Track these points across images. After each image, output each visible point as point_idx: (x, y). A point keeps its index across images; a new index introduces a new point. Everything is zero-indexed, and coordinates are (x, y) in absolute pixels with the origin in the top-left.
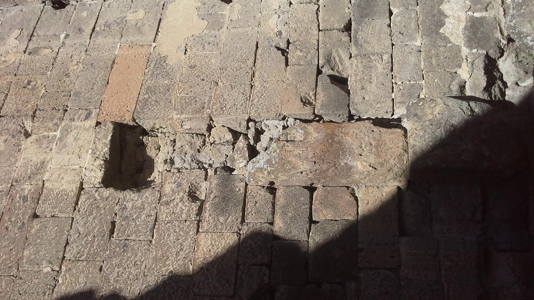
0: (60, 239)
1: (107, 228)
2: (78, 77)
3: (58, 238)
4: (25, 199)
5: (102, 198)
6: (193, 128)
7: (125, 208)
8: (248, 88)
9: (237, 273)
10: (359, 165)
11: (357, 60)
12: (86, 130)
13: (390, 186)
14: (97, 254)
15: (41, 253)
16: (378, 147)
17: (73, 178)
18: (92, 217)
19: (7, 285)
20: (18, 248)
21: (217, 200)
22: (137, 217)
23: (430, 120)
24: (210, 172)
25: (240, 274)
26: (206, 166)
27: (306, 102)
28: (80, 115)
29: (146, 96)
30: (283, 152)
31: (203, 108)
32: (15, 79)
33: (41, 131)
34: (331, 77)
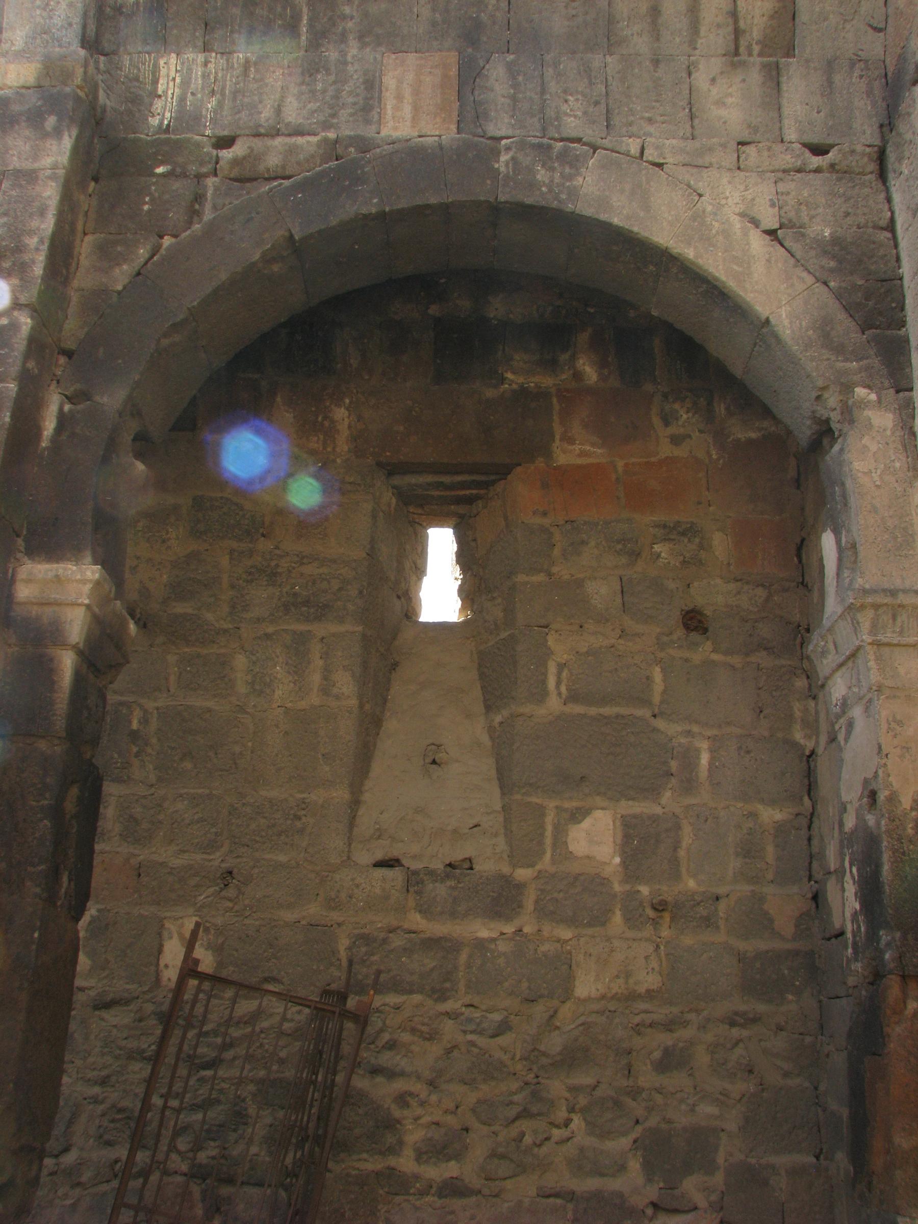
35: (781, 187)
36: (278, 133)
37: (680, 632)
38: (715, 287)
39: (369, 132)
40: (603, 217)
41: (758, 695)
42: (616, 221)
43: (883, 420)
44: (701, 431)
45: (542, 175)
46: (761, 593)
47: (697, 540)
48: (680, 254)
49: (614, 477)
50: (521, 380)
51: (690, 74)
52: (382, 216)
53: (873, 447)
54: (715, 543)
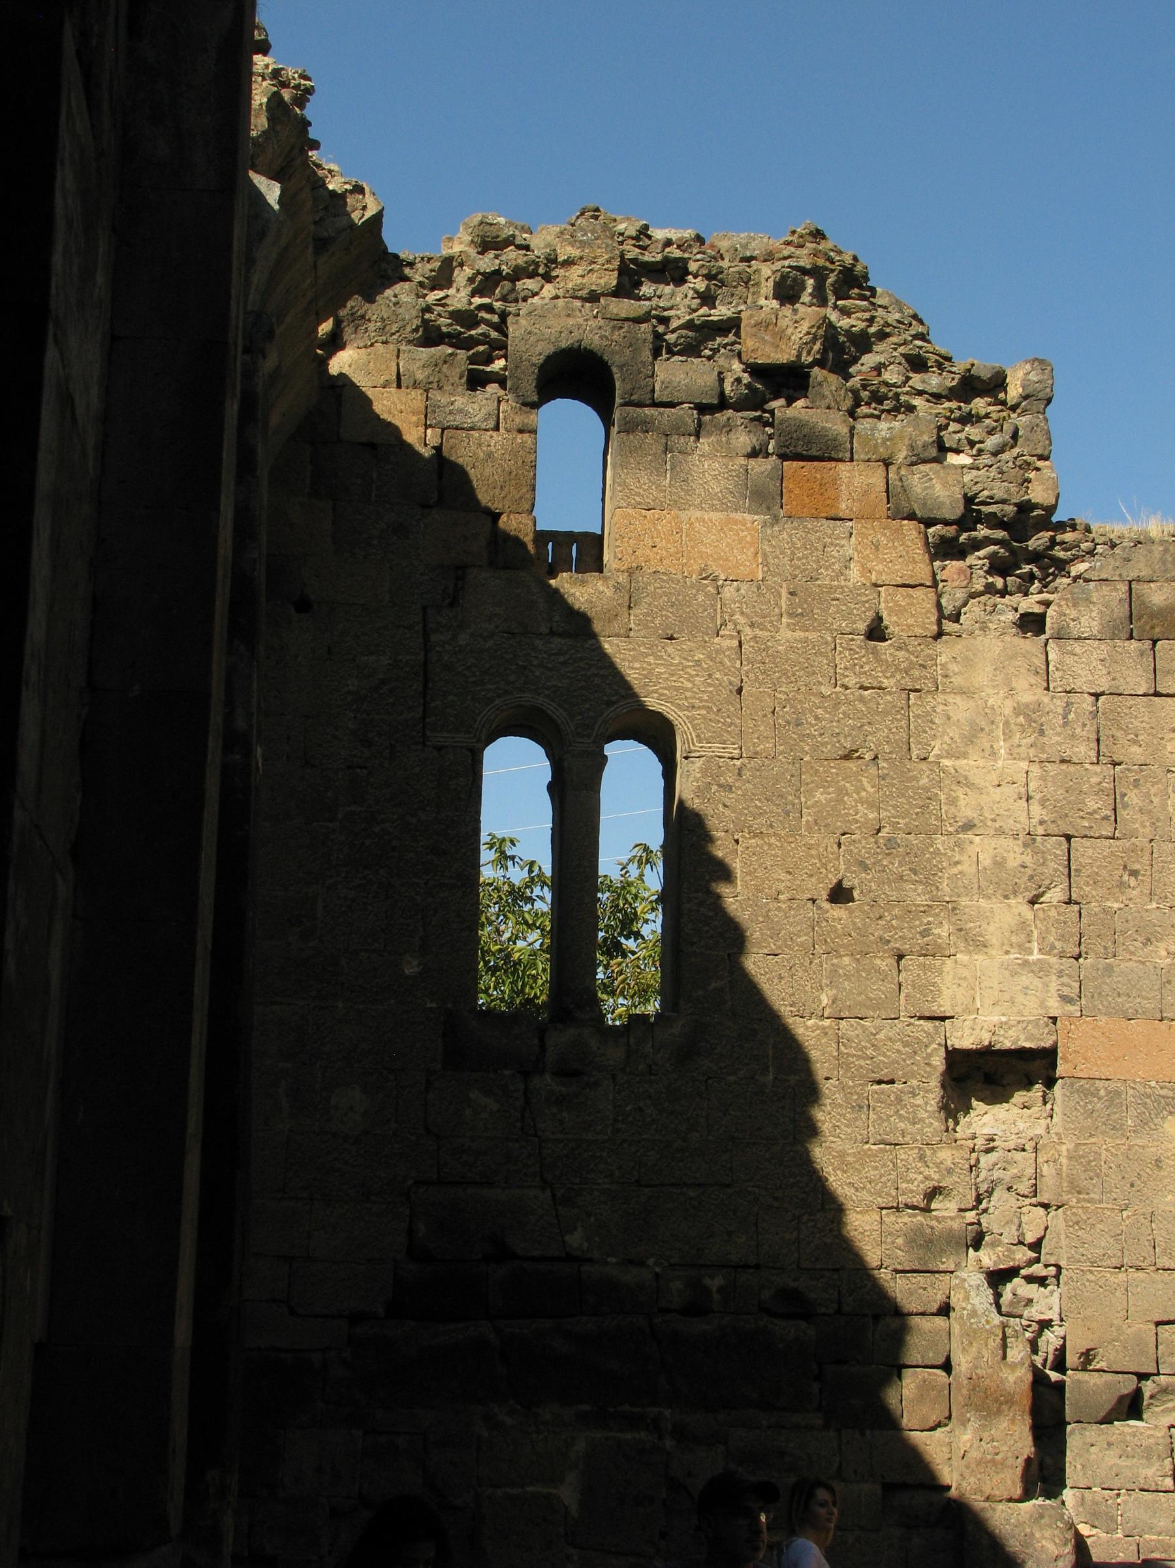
1: (885, 1075)
2: (1143, 963)
3: (869, 1003)
4: (925, 933)
5: (929, 1055)
6: (1044, 1179)
7: (914, 1095)
8: (1115, 1262)
9: (828, 1270)
10: (966, 1437)
11: (1163, 1437)
12: (1042, 1003)
13: (949, 1475)
14: (848, 1069)
16: (993, 1464)
17: (959, 1002)
18: (901, 1048)
19: (801, 945)
21: (928, 1231)
22: (901, 1116)
23: (1033, 1534)
24: (971, 1216)
25: (827, 1274)
26: (984, 1205)
27: (1087, 1357)
28: (1069, 986)
29: (1102, 1093)
30: (985, 1334)
31: (1079, 1193)
32: (1142, 841)
33: (1039, 925)
34: (1137, 1394)
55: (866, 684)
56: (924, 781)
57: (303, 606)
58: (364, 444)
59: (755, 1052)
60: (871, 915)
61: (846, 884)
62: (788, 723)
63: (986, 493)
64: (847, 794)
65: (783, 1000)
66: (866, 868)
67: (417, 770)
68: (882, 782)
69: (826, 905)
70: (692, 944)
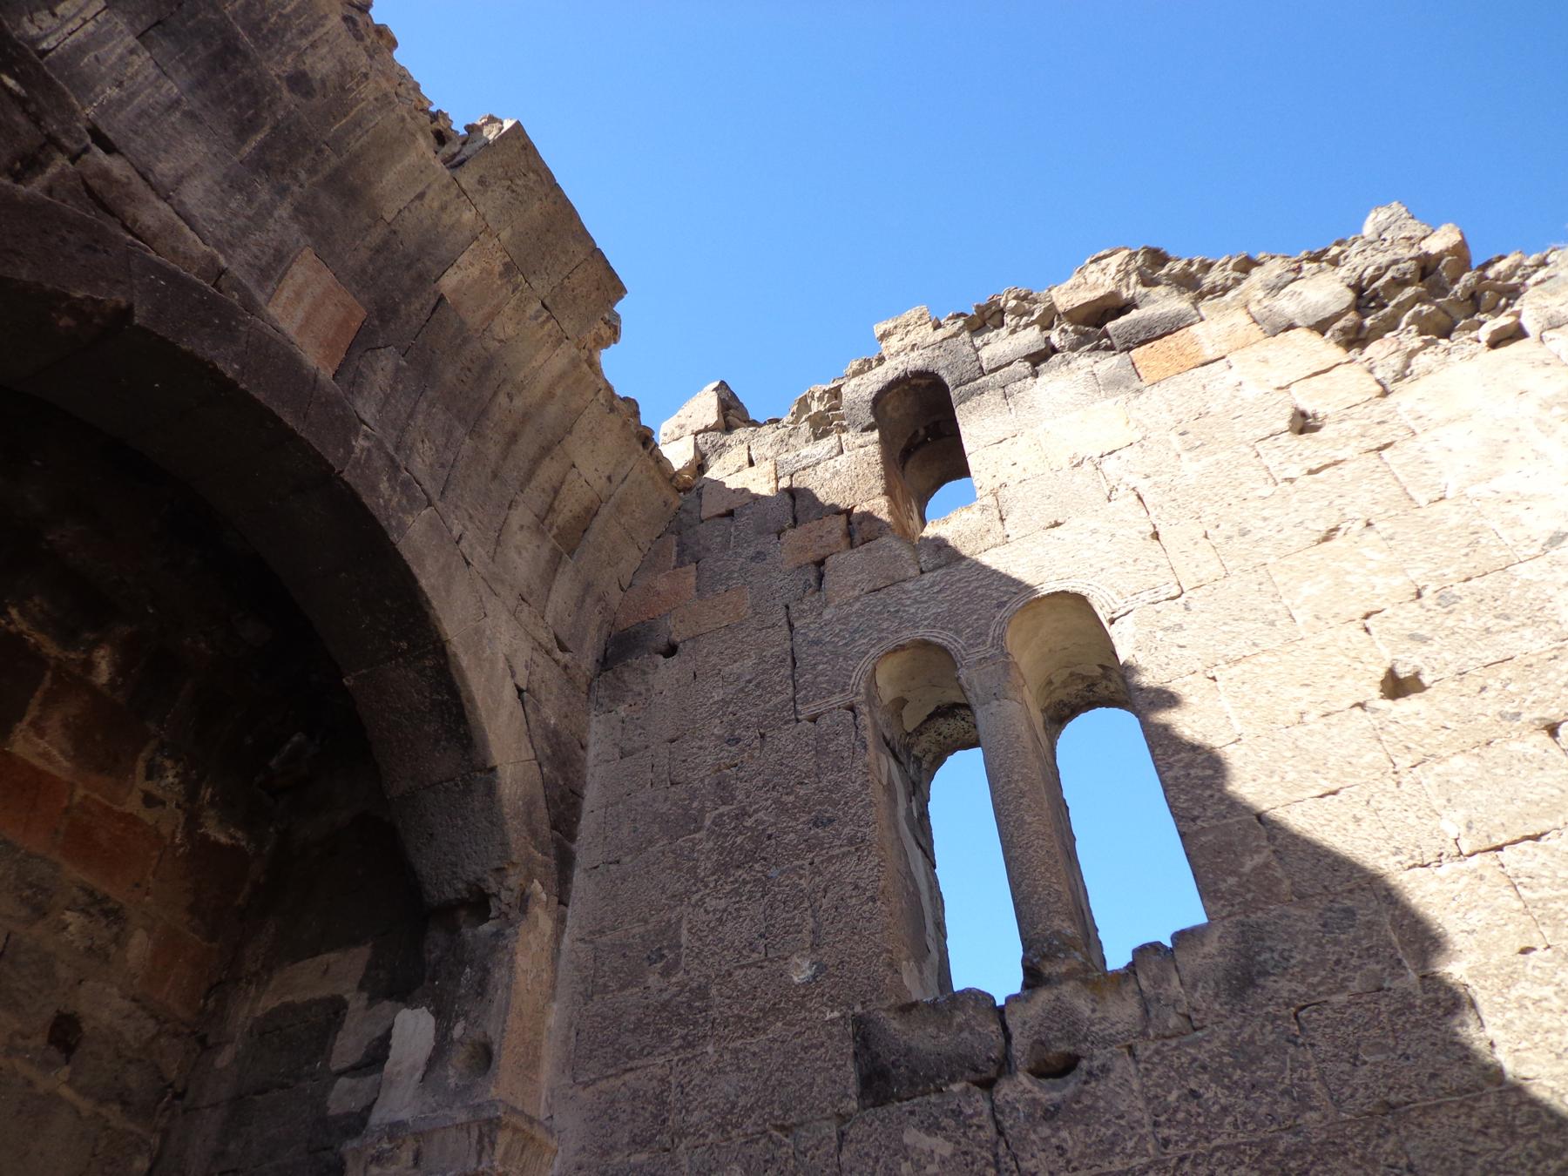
0: (1537, 817)
3: (1535, 810)
15: (1476, 792)
20: (1456, 739)
35: (536, 656)
36: (166, 199)
37: (40, 1040)
38: (460, 706)
39: (260, 297)
40: (415, 570)
41: (89, 1164)
42: (423, 582)
43: (546, 924)
44: (178, 806)
45: (384, 486)
46: (151, 1026)
47: (115, 929)
48: (455, 655)
49: (66, 803)
50: (24, 627)
51: (510, 507)
52: (231, 385)
53: (534, 947)
54: (134, 941)
55: (1315, 467)
56: (1454, 520)
57: (671, 650)
58: (722, 516)
59: (1365, 943)
60: (1465, 691)
61: (1403, 672)
62: (1229, 538)
63: (1370, 271)
64: (1348, 573)
65: (1377, 850)
66: (1424, 640)
67: (791, 747)
68: (1391, 543)
69: (1389, 703)
70: (1194, 819)
